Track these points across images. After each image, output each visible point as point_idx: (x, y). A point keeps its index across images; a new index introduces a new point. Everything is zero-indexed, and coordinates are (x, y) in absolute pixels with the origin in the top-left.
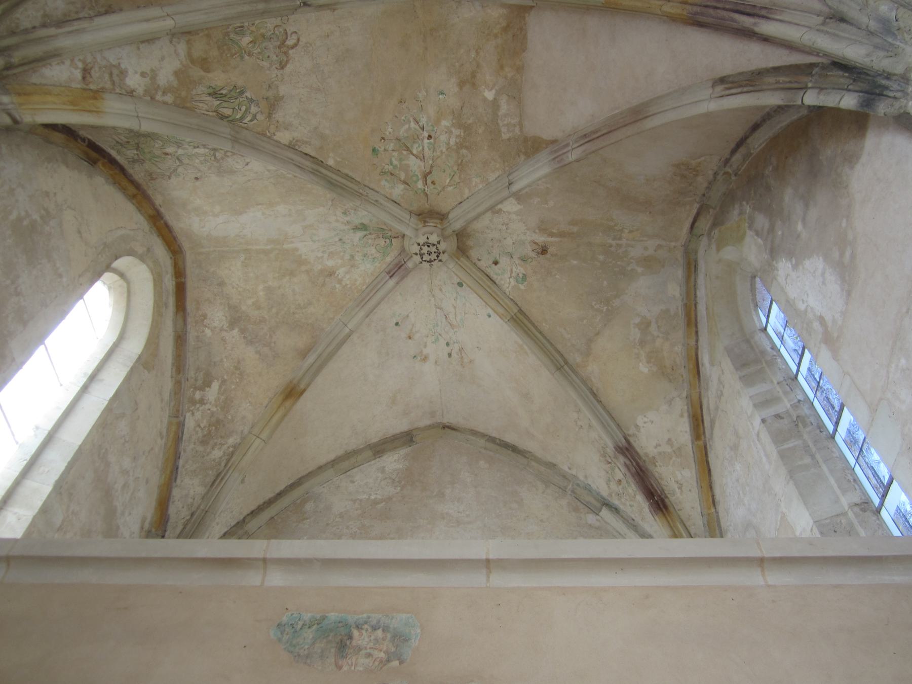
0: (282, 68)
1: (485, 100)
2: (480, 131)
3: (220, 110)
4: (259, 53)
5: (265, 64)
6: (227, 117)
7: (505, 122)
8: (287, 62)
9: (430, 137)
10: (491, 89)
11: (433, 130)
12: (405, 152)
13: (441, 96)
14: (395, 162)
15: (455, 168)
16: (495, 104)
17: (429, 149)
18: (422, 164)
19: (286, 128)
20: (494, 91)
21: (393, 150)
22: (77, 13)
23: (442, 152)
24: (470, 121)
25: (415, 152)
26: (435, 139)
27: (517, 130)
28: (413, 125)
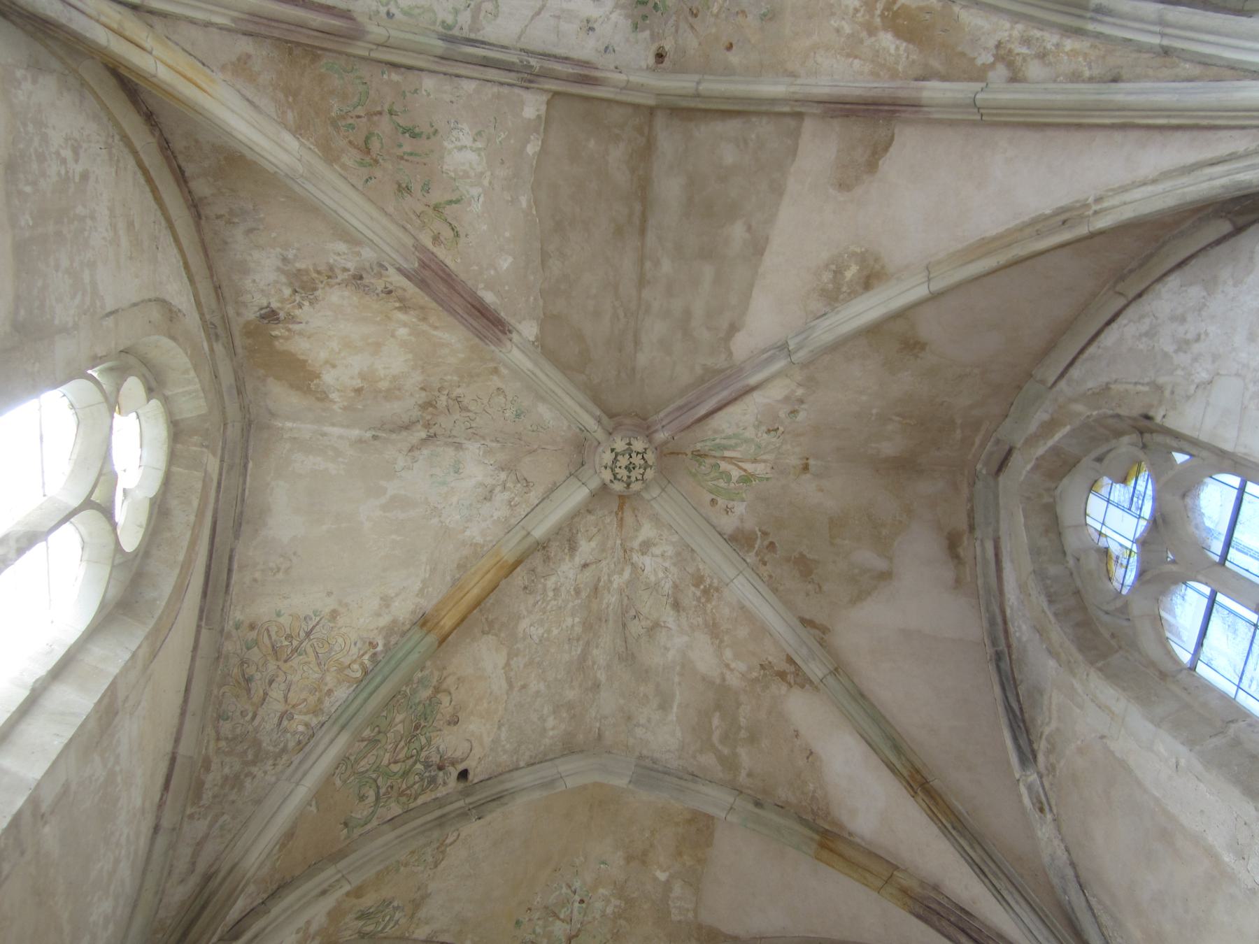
0: (436, 866)
1: (655, 879)
2: (646, 907)
3: (364, 929)
4: (416, 860)
5: (421, 868)
6: (367, 934)
7: (678, 905)
8: (443, 860)
9: (582, 901)
10: (664, 871)
11: (587, 895)
12: (551, 919)
13: (602, 866)
14: (538, 930)
15: (609, 936)
16: (667, 885)
17: (580, 913)
18: (568, 927)
19: (427, 923)
20: (667, 874)
21: (539, 919)
22: (251, 903)
23: (594, 918)
24: (634, 895)
25: (562, 916)
26: (589, 904)
27: (691, 915)
28: (564, 890)
